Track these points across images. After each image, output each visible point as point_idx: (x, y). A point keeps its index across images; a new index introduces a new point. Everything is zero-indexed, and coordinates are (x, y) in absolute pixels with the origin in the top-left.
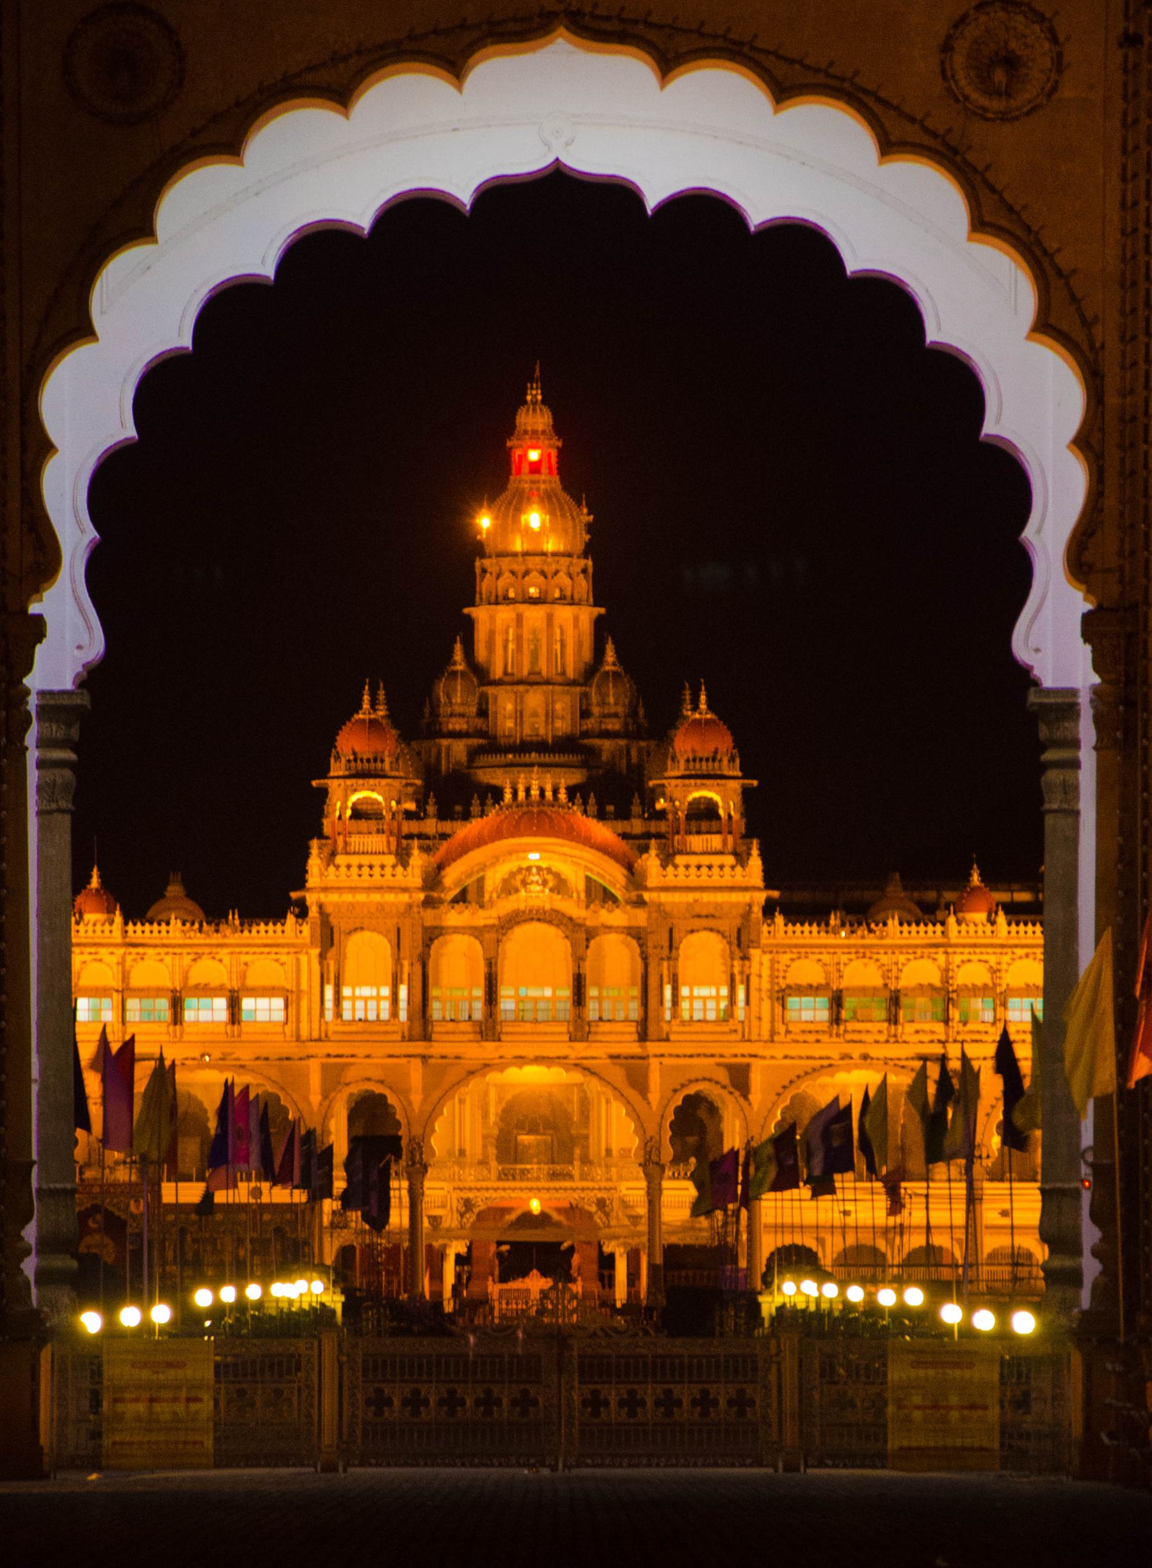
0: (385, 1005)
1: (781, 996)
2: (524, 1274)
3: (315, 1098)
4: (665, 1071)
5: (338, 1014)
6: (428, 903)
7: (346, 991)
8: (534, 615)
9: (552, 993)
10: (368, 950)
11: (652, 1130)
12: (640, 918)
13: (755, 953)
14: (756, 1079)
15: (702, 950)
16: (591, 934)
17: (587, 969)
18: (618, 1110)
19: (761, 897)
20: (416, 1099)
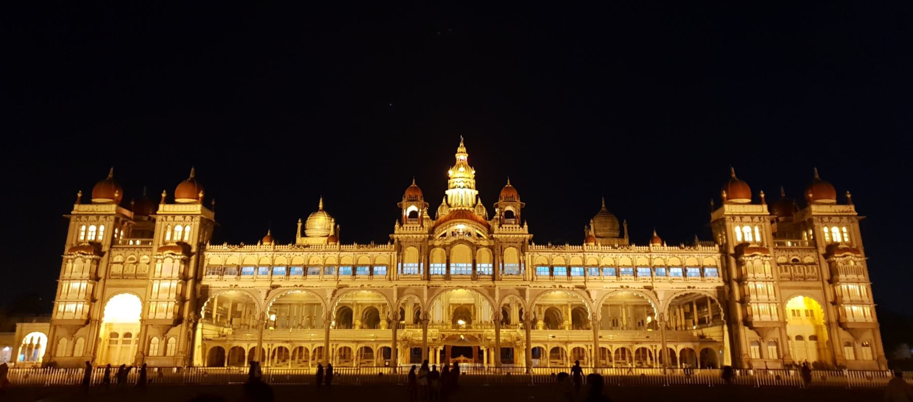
0: (417, 269)
1: (534, 267)
2: (459, 356)
3: (395, 299)
4: (501, 291)
5: (402, 272)
6: (430, 238)
7: (405, 265)
8: (462, 191)
9: (466, 267)
10: (412, 252)
11: (496, 308)
12: (492, 243)
13: (527, 253)
14: (528, 293)
15: (511, 254)
16: (478, 247)
17: (477, 258)
18: (486, 303)
19: (528, 236)
20: (425, 299)
